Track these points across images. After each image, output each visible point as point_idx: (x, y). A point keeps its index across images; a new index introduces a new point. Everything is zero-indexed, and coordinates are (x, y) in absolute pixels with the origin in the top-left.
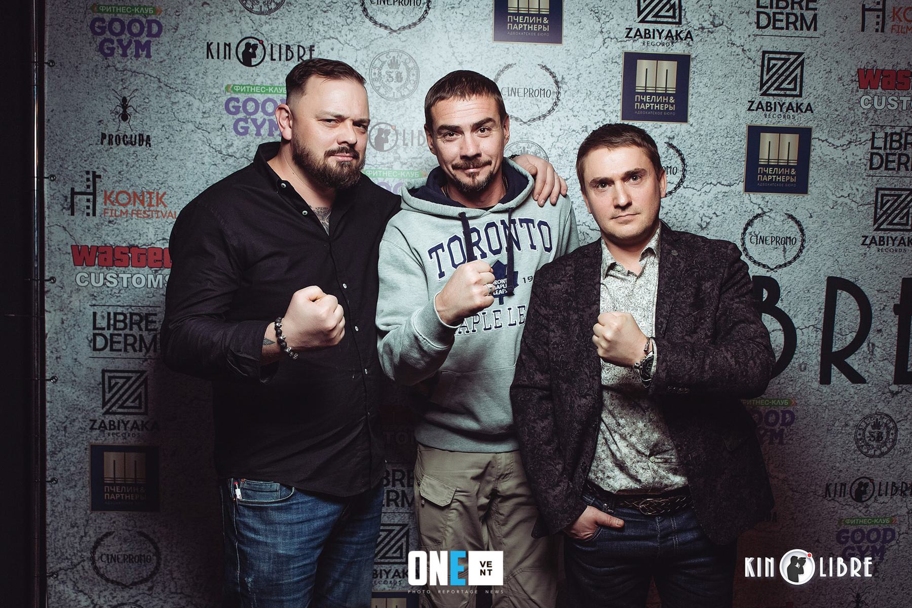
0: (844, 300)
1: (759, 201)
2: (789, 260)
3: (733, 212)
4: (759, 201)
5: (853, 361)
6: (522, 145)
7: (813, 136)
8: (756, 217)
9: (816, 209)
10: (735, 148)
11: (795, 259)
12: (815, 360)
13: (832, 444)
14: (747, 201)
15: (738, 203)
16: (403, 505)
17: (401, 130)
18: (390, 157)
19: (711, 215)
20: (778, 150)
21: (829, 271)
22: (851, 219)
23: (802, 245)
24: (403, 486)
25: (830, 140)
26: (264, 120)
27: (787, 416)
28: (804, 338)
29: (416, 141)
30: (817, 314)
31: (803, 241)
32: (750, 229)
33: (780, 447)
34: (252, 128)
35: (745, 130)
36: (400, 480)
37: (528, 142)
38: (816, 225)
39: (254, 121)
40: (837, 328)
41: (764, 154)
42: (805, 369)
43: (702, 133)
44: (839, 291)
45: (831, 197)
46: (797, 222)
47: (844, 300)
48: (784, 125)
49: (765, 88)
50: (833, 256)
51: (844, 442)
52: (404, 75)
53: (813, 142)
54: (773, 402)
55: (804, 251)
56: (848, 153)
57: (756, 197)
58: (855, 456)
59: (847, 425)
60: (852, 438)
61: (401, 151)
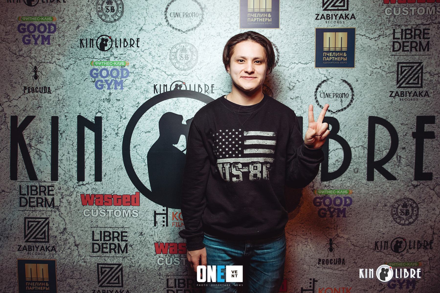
0: (380, 130)
1: (325, 72)
2: (345, 107)
3: (309, 80)
4: (325, 72)
5: (387, 167)
6: (182, 45)
7: (356, 33)
8: (323, 82)
9: (360, 76)
10: (308, 42)
11: (348, 106)
12: (364, 166)
13: (377, 217)
14: (317, 73)
15: (311, 74)
16: (119, 252)
17: (114, 39)
18: (108, 54)
19: (296, 82)
20: (335, 42)
21: (370, 113)
22: (382, 81)
23: (352, 98)
24: (118, 240)
25: (367, 35)
26: (39, 36)
27: (348, 200)
28: (356, 153)
29: (122, 45)
30: (363, 138)
31: (353, 95)
32: (320, 89)
33: (344, 219)
34: (33, 40)
35: (314, 31)
36: (117, 237)
37: (186, 43)
38: (360, 86)
39: (34, 36)
40: (376, 147)
41: (326, 45)
42: (357, 172)
43: (288, 34)
44: (376, 125)
45: (369, 68)
46: (349, 84)
47: (380, 130)
48: (337, 27)
50: (372, 104)
51: (385, 216)
53: (357, 37)
54: (338, 192)
55: (353, 101)
56: (379, 42)
57: (323, 70)
58: (392, 224)
59: (386, 205)
60: (389, 213)
61: (114, 51)
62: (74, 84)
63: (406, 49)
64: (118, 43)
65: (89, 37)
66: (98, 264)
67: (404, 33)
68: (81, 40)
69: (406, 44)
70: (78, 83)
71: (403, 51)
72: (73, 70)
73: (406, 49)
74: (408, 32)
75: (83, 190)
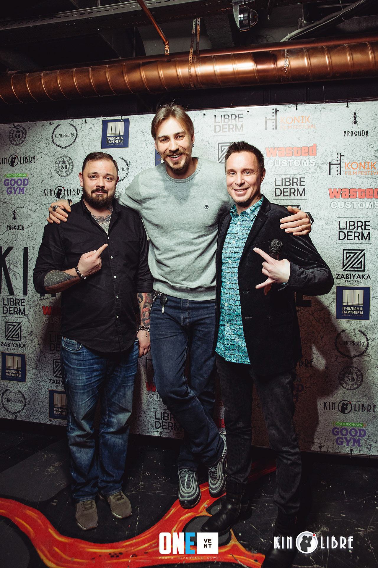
29: (72, 193)
49: (220, 160)
52: (68, 166)
62: (39, 223)
63: (286, 194)
64: (69, 192)
65: (49, 188)
66: (54, 359)
67: (284, 181)
68: (44, 191)
69: (285, 190)
70: (41, 222)
71: (284, 196)
72: (39, 213)
73: (286, 194)
74: (287, 180)
75: (44, 303)
